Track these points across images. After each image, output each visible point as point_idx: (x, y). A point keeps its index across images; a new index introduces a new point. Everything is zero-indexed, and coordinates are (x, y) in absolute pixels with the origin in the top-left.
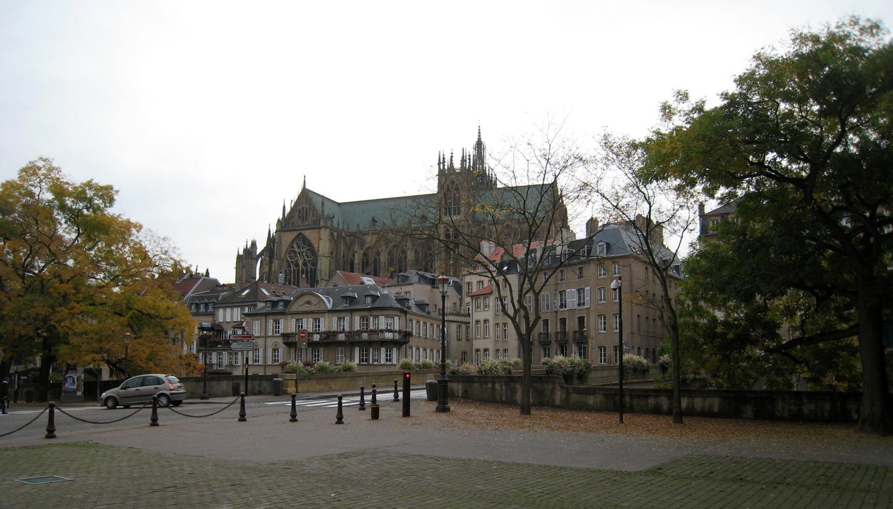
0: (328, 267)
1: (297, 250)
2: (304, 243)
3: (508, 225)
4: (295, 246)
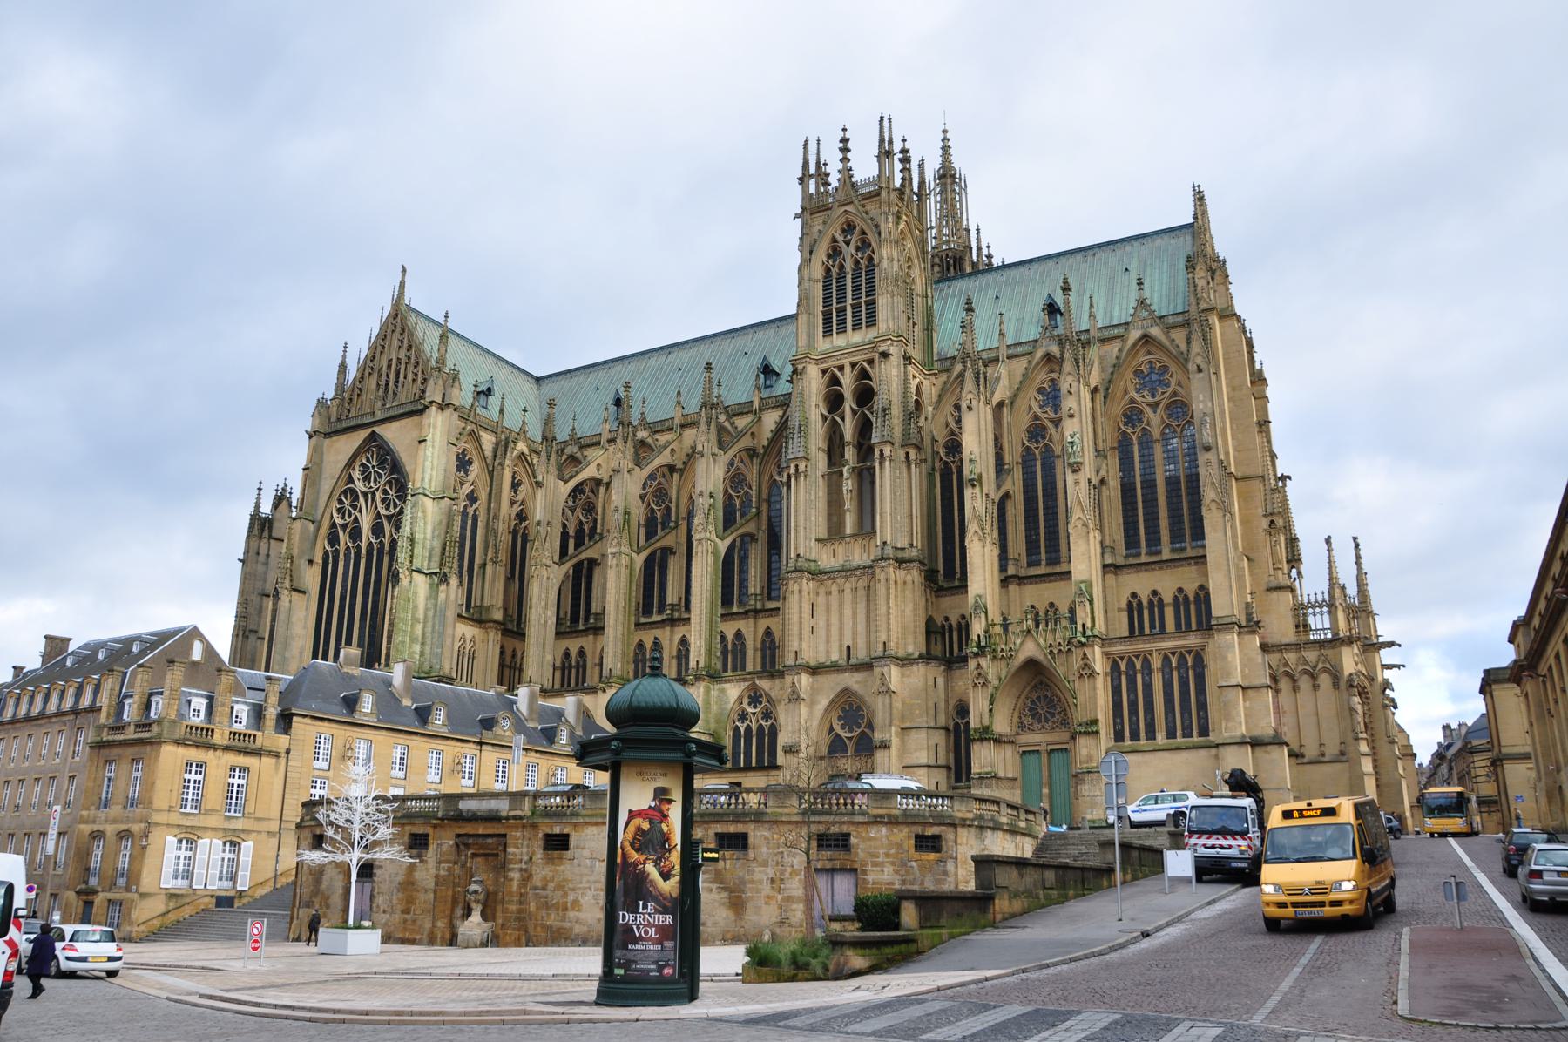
1: (360, 486)
2: (382, 463)
3: (1048, 357)
4: (356, 475)
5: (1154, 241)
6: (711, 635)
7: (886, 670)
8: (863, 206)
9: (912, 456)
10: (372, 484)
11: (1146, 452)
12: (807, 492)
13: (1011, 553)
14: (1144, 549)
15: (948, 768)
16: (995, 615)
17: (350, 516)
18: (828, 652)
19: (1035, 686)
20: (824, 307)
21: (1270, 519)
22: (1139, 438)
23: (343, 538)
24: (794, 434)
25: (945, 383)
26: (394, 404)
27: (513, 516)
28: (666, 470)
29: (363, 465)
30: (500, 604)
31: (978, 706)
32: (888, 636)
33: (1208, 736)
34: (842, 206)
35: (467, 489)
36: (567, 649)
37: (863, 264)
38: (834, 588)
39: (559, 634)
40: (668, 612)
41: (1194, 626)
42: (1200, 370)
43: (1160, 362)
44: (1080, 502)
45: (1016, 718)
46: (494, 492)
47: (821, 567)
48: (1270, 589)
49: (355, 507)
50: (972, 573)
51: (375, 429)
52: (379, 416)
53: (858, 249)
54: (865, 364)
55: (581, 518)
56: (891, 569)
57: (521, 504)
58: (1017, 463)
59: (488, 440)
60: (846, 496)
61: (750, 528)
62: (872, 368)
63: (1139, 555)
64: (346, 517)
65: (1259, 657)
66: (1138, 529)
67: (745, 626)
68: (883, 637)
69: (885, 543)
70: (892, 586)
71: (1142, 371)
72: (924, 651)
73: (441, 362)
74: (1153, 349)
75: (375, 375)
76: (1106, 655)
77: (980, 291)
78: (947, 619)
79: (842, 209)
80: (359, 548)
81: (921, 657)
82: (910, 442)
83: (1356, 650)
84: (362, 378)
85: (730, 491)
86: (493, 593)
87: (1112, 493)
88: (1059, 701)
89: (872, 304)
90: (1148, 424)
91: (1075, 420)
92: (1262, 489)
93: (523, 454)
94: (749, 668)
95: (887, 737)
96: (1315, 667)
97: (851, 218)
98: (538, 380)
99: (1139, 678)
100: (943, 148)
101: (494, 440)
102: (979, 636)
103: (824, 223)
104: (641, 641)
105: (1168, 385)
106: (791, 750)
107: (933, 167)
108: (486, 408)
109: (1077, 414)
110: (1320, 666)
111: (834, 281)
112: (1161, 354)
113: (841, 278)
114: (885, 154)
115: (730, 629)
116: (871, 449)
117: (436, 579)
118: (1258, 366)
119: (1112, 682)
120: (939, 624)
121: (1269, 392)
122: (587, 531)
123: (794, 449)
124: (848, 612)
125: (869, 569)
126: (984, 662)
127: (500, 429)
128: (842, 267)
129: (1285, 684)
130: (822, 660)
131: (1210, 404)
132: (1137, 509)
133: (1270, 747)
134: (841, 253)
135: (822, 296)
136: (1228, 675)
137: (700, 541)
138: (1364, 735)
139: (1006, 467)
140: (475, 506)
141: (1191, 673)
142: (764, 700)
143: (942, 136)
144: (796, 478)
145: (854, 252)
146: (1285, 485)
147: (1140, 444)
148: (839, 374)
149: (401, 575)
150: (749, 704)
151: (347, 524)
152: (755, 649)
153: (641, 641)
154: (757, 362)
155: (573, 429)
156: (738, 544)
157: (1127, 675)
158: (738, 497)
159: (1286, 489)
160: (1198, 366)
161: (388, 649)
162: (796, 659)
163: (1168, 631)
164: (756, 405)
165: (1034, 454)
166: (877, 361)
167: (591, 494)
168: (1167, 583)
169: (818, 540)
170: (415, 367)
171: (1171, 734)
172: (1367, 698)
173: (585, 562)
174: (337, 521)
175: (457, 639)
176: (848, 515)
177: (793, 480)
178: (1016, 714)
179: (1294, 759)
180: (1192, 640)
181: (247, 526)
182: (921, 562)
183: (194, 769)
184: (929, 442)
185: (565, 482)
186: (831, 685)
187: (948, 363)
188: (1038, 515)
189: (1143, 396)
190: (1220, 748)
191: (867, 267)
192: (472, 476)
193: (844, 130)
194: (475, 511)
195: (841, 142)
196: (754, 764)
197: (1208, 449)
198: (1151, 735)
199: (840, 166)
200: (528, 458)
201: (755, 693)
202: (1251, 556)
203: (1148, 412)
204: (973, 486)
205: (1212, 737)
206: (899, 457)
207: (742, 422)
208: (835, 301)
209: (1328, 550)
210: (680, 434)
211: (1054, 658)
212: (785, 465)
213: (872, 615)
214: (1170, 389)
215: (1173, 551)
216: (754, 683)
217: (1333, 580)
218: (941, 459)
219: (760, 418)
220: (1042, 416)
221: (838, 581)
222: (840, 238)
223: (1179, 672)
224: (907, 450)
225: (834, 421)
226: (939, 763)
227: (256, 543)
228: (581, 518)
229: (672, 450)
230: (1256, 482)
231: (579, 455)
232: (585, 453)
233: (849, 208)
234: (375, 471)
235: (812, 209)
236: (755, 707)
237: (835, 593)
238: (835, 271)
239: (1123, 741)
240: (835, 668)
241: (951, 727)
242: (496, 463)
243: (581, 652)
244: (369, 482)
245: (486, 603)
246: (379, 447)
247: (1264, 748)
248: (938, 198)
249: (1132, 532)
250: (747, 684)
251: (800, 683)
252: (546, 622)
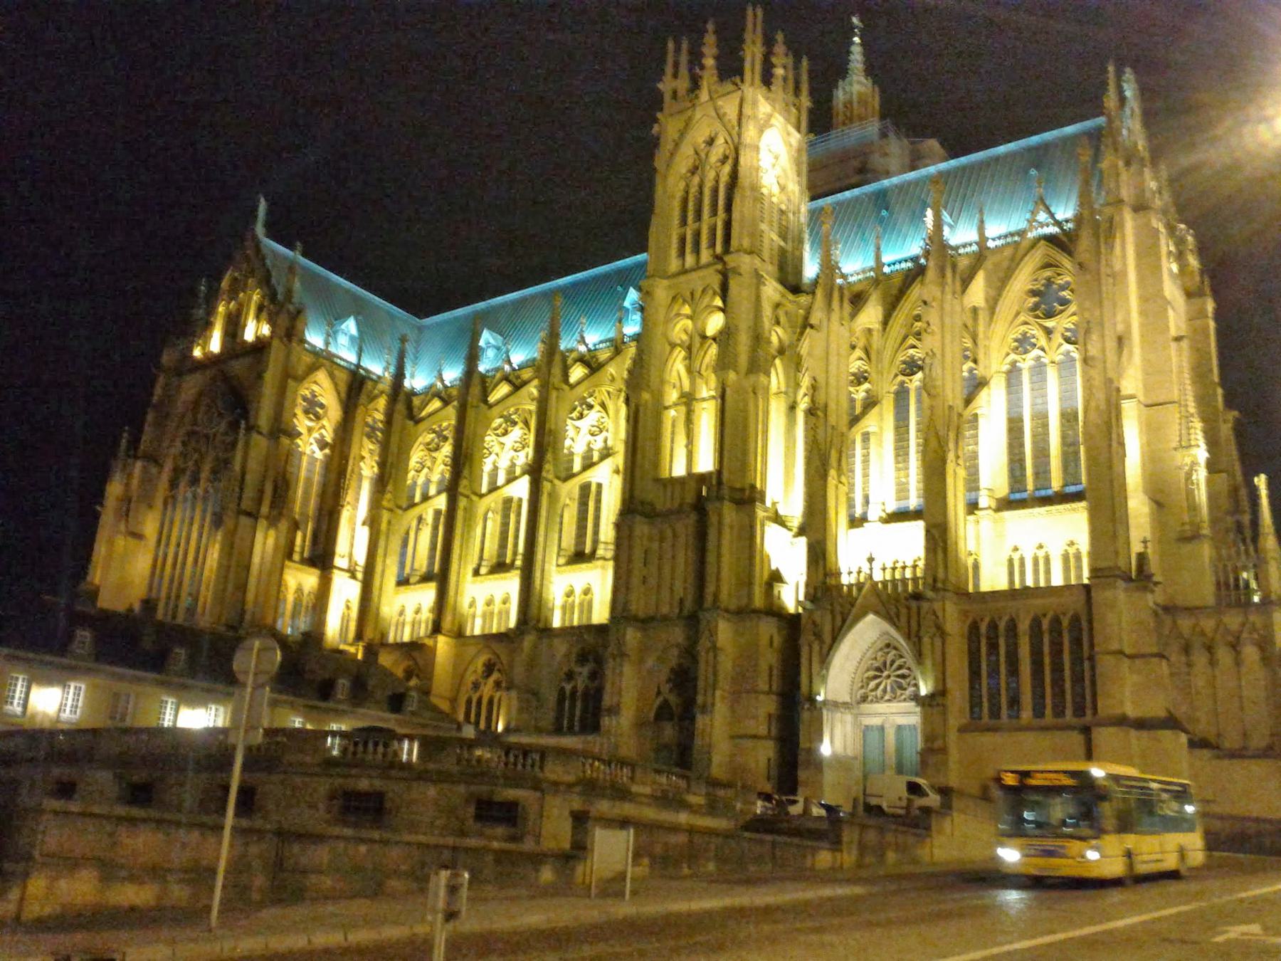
19: (881, 649)
38: (669, 533)
96: (1238, 638)
110: (1245, 635)
171: (1039, 712)
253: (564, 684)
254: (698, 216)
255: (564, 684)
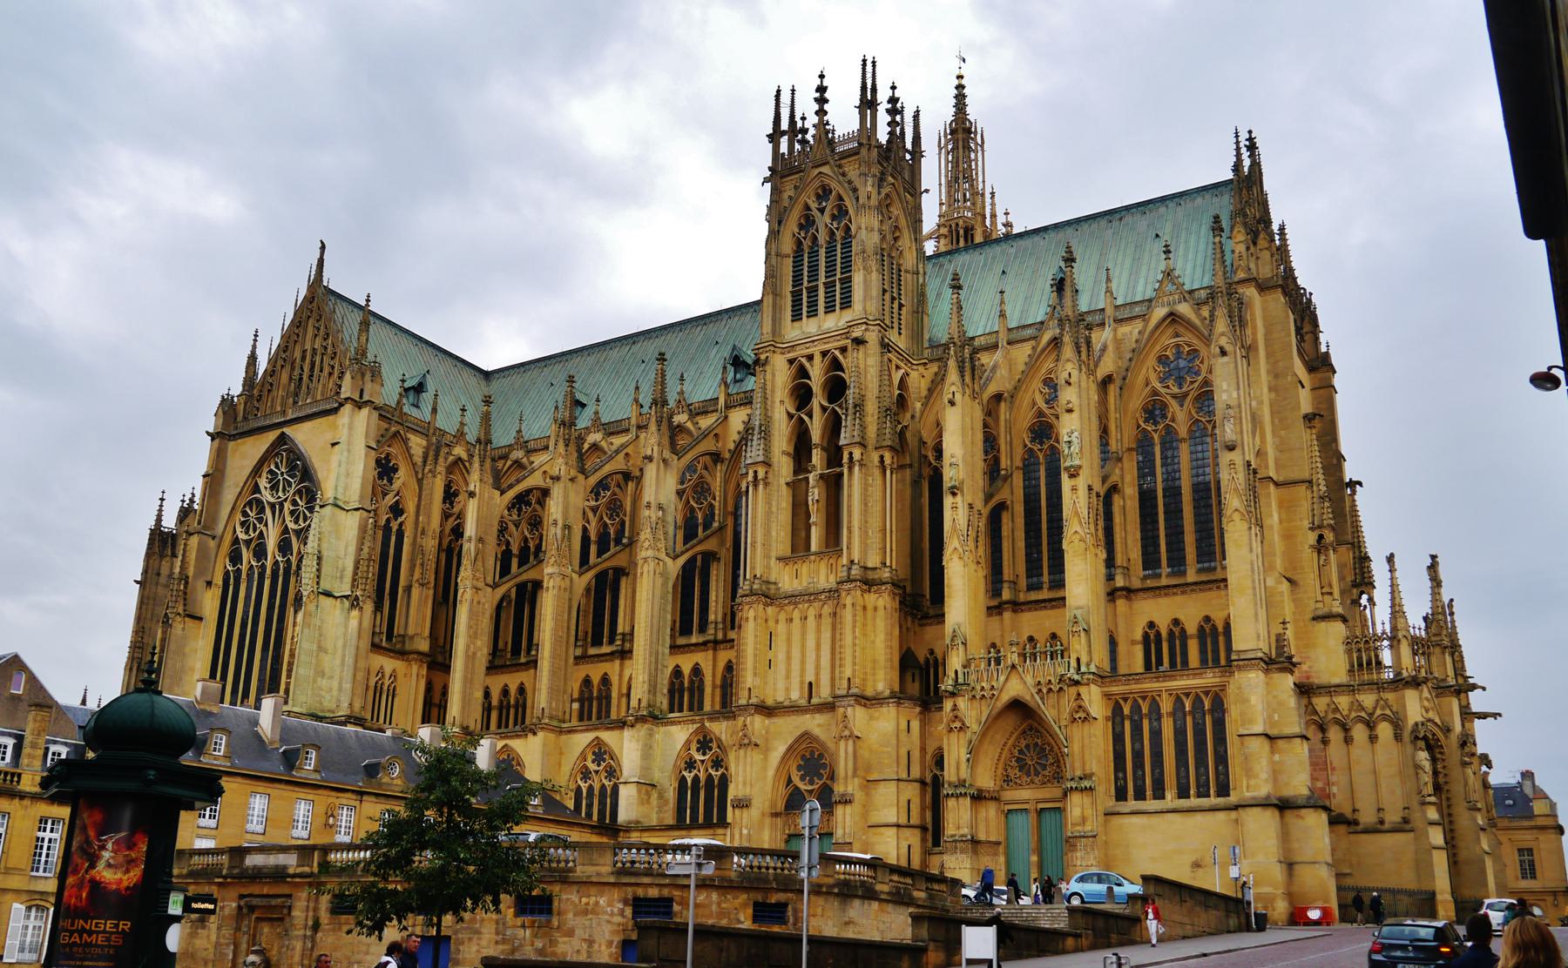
0: (352, 549)
1: (267, 496)
2: (292, 469)
4: (263, 483)
5: (1195, 199)
6: (656, 669)
7: (849, 709)
8: (840, 166)
9: (888, 460)
10: (280, 494)
11: (1169, 453)
12: (769, 503)
13: (1007, 574)
14: (1165, 570)
15: (923, 828)
16: (978, 650)
17: (255, 531)
18: (788, 690)
19: (1024, 732)
20: (794, 286)
21: (1317, 533)
22: (1161, 437)
23: (246, 555)
24: (753, 434)
25: (936, 374)
26: (308, 401)
27: (447, 530)
28: (620, 477)
29: (271, 472)
30: (427, 632)
31: (956, 753)
32: (854, 671)
33: (1229, 795)
34: (817, 167)
35: (390, 500)
36: (506, 685)
37: (839, 235)
38: (796, 615)
39: (493, 668)
40: (618, 643)
41: (1223, 662)
42: (1223, 353)
43: (1190, 346)
44: (1077, 513)
45: (1000, 771)
46: (423, 503)
47: (781, 590)
48: (1314, 619)
49: (260, 520)
50: (950, 597)
51: (285, 430)
52: (290, 415)
53: (834, 218)
54: (837, 353)
55: (526, 533)
56: (859, 593)
57: (458, 517)
58: (1017, 468)
59: (417, 443)
60: (812, 508)
61: (710, 545)
62: (845, 358)
63: (1160, 576)
64: (251, 532)
65: (1292, 701)
66: (1159, 545)
67: (704, 659)
68: (848, 673)
69: (852, 562)
70: (860, 613)
71: (1167, 357)
72: (897, 688)
73: (362, 352)
74: (1181, 330)
75: (288, 367)
76: (1107, 696)
77: (985, 265)
78: (932, 652)
79: (816, 171)
80: (263, 567)
81: (893, 695)
82: (885, 443)
83: (1426, 694)
84: (274, 371)
85: (692, 503)
86: (417, 617)
87: (1129, 503)
88: (1051, 750)
89: (847, 282)
90: (1173, 420)
91: (1075, 415)
92: (1310, 496)
93: (460, 459)
94: (707, 707)
95: (850, 790)
96: (1371, 715)
97: (827, 181)
98: (487, 375)
99: (1146, 723)
100: (956, 97)
101: (424, 443)
102: (956, 672)
103: (796, 187)
104: (588, 676)
105: (1197, 373)
106: (743, 804)
107: (936, 122)
108: (418, 407)
109: (1076, 409)
111: (806, 255)
112: (1190, 335)
113: (814, 253)
114: (868, 104)
115: (686, 663)
116: (839, 449)
117: (347, 604)
118: (1323, 349)
119: (1113, 728)
120: (921, 659)
121: (1337, 381)
122: (532, 549)
123: (754, 453)
124: (811, 643)
125: (833, 594)
126: (962, 703)
127: (431, 431)
128: (815, 239)
129: (1335, 734)
130: (780, 699)
131: (1235, 395)
132: (1157, 522)
133: (1303, 811)
134: (814, 221)
135: (791, 274)
136: (1251, 721)
137: (645, 559)
138: (1433, 799)
139: (1003, 472)
140: (400, 520)
141: (1208, 719)
142: (714, 745)
143: (956, 82)
144: (756, 485)
145: (828, 221)
146: (1354, 492)
147: (1163, 444)
148: (807, 365)
149: (304, 599)
150: (698, 750)
151: (251, 540)
152: (714, 687)
153: (588, 676)
154: (726, 352)
155: (519, 431)
156: (699, 563)
157: (1132, 721)
158: (700, 509)
159: (1356, 498)
160: (1221, 348)
161: (288, 684)
162: (750, 698)
163: (1191, 667)
164: (722, 401)
165: (1038, 458)
166: (850, 348)
167: (538, 507)
168: (1189, 610)
169: (779, 559)
170: (332, 358)
171: (1183, 793)
172: (1441, 753)
173: (529, 585)
174: (240, 537)
175: (373, 674)
176: (813, 529)
177: (751, 489)
178: (1001, 766)
179: (1342, 829)
180: (1210, 679)
181: (146, 542)
182: (893, 584)
183: (49, 826)
184: (916, 444)
185: (502, 493)
186: (786, 730)
187: (941, 349)
188: (1040, 529)
189: (1168, 387)
190: (1239, 809)
191: (844, 238)
192: (397, 484)
193: (822, 76)
194: (401, 524)
195: (817, 91)
196: (701, 820)
197: (1231, 448)
198: (1159, 794)
199: (815, 120)
200: (467, 464)
201: (705, 737)
202: (1295, 578)
203: (1174, 405)
204: (954, 494)
205: (1233, 798)
206: (872, 462)
207: (705, 422)
208: (806, 279)
209: (1390, 571)
210: (637, 437)
211: (1042, 699)
212: (744, 471)
213: (837, 646)
214: (1200, 378)
215: (1200, 571)
216: (703, 724)
217: (1397, 611)
218: (930, 464)
219: (726, 417)
220: (1047, 412)
221: (801, 606)
222: (814, 205)
223: (1194, 718)
224: (881, 453)
225: (801, 420)
226: (912, 822)
227: (157, 562)
228: (526, 533)
229: (627, 454)
230: (1302, 489)
231: (525, 460)
232: (532, 459)
233: (825, 169)
234: (284, 479)
235: (780, 172)
236: (704, 754)
237: (797, 621)
238: (806, 244)
239: (1126, 800)
240: (793, 709)
241: (928, 780)
242: (426, 470)
243: (521, 690)
244: (277, 491)
245: (411, 631)
246: (289, 451)
247: (1296, 812)
248: (950, 158)
249: (1151, 549)
250: (696, 726)
251: (752, 723)
252: (475, 654)
253: (685, 773)
254: (813, 275)
255: (684, 773)
